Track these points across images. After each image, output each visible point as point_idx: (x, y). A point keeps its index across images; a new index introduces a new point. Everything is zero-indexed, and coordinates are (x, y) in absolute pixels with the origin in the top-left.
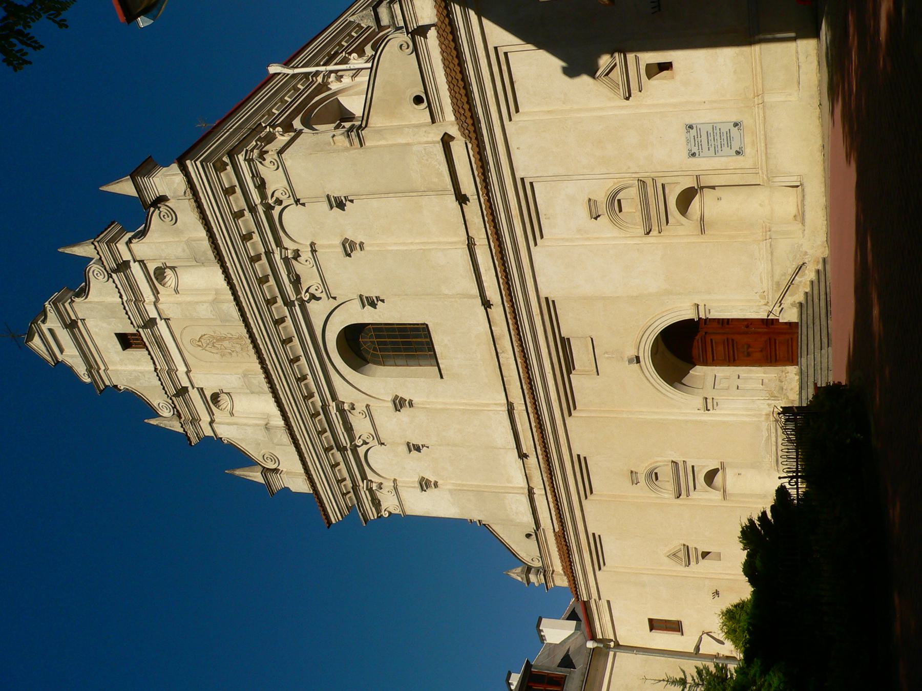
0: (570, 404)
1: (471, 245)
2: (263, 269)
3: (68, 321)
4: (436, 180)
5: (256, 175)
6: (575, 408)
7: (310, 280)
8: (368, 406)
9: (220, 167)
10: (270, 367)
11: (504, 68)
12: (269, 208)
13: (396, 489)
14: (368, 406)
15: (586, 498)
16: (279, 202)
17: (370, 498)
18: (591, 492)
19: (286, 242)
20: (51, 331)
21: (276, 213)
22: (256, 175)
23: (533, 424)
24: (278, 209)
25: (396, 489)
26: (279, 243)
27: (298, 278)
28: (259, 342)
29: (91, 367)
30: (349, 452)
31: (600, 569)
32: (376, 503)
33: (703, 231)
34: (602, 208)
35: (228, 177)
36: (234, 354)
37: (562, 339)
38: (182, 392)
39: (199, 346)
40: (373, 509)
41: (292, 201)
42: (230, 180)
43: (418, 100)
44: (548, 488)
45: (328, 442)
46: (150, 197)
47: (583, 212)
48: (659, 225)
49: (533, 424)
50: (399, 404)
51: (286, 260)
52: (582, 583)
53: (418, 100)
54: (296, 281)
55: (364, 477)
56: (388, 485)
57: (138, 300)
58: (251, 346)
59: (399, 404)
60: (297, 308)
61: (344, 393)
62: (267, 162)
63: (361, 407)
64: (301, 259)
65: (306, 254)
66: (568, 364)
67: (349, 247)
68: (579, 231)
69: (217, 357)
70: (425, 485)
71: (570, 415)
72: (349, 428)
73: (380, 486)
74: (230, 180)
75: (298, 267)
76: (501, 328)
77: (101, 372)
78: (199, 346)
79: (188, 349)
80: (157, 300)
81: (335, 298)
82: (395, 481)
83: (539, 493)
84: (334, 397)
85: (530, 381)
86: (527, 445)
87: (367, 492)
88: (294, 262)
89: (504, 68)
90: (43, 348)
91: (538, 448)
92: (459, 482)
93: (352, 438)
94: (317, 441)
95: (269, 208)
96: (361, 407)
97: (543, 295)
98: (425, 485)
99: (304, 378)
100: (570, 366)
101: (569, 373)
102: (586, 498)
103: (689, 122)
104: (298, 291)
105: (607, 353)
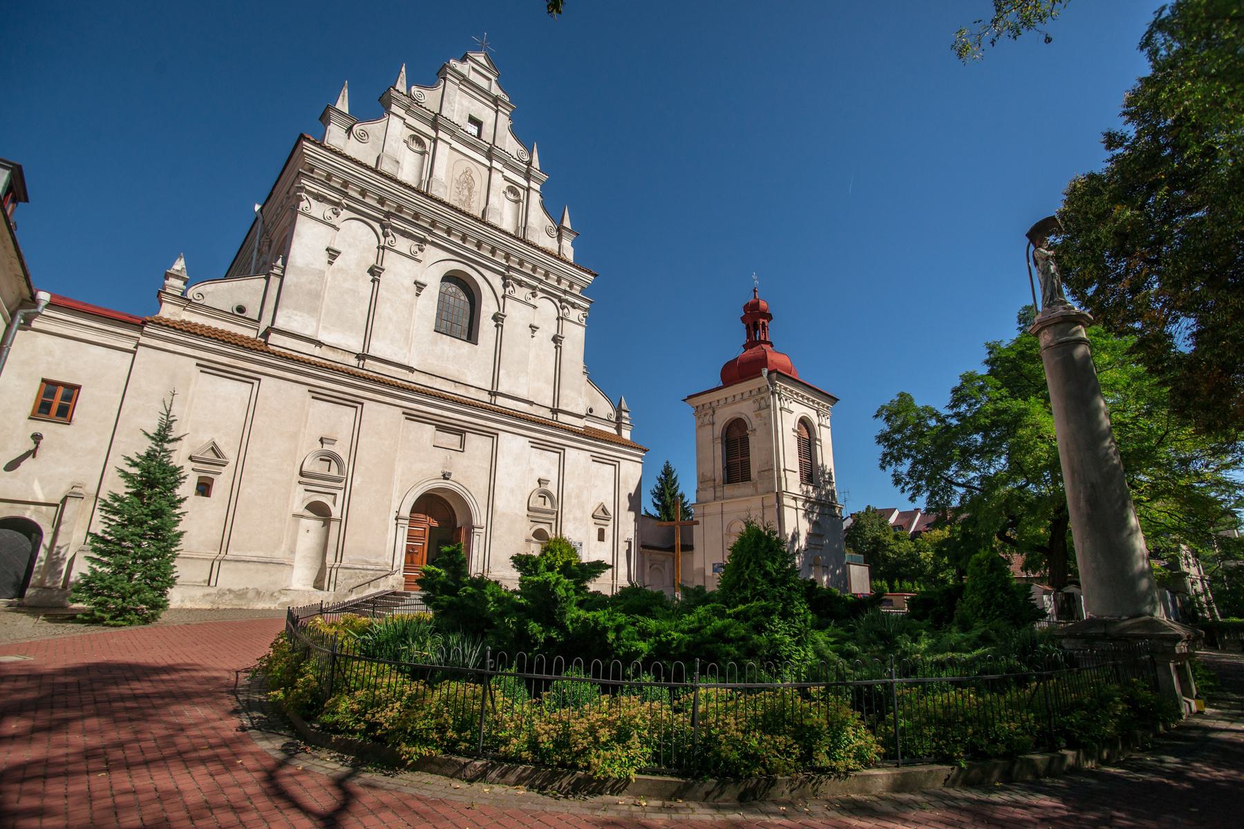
0: (411, 416)
1: (531, 403)
2: (527, 268)
3: (499, 103)
4: (565, 401)
5: (579, 307)
6: (406, 418)
7: (522, 293)
8: (420, 261)
9: (583, 290)
10: (469, 220)
11: (610, 462)
12: (561, 301)
13: (334, 226)
14: (420, 261)
15: (309, 391)
16: (563, 308)
17: (328, 197)
18: (313, 398)
19: (540, 294)
20: (489, 79)
21: (556, 301)
22: (579, 307)
23: (399, 382)
24: (559, 304)
25: (334, 226)
26: (542, 291)
27: (521, 286)
28: (489, 229)
29: (464, 80)
30: (382, 217)
31: (197, 365)
32: (320, 198)
33: (527, 541)
34: (543, 487)
35: (576, 290)
36: (458, 191)
37: (465, 432)
38: (435, 125)
39: (467, 172)
40: (316, 191)
41: (561, 315)
42: (576, 290)
43: (591, 410)
44: (328, 363)
45: (389, 205)
46: (565, 233)
47: (543, 476)
48: (532, 517)
49: (399, 382)
50: (420, 286)
51: (534, 288)
52: (187, 339)
53: (591, 410)
54: (520, 283)
55: (349, 208)
56: (335, 221)
57: (507, 165)
58: (463, 209)
59: (420, 286)
60: (503, 270)
61: (432, 253)
62: (581, 317)
63: (419, 256)
64: (530, 296)
65: (532, 301)
66: (443, 427)
67: (533, 328)
68: (532, 470)
69: (457, 177)
70: (333, 254)
71: (404, 413)
72: (404, 234)
73: (337, 214)
74: (576, 290)
75: (526, 292)
76: (473, 394)
77: (458, 82)
78: (467, 172)
79: (468, 164)
80: (503, 176)
81: (504, 297)
82: (338, 229)
83: (317, 351)
84: (433, 244)
85: (445, 399)
86: (370, 364)
87: (337, 200)
88: (531, 291)
89: (610, 462)
90: (477, 58)
91: (375, 375)
92: (328, 284)
93: (395, 229)
94: (394, 199)
95: (561, 301)
96: (419, 256)
97: (500, 433)
98: (333, 254)
99: (449, 231)
100: (440, 428)
101: (437, 426)
102: (309, 391)
103: (583, 544)
104: (514, 279)
105: (451, 458)
